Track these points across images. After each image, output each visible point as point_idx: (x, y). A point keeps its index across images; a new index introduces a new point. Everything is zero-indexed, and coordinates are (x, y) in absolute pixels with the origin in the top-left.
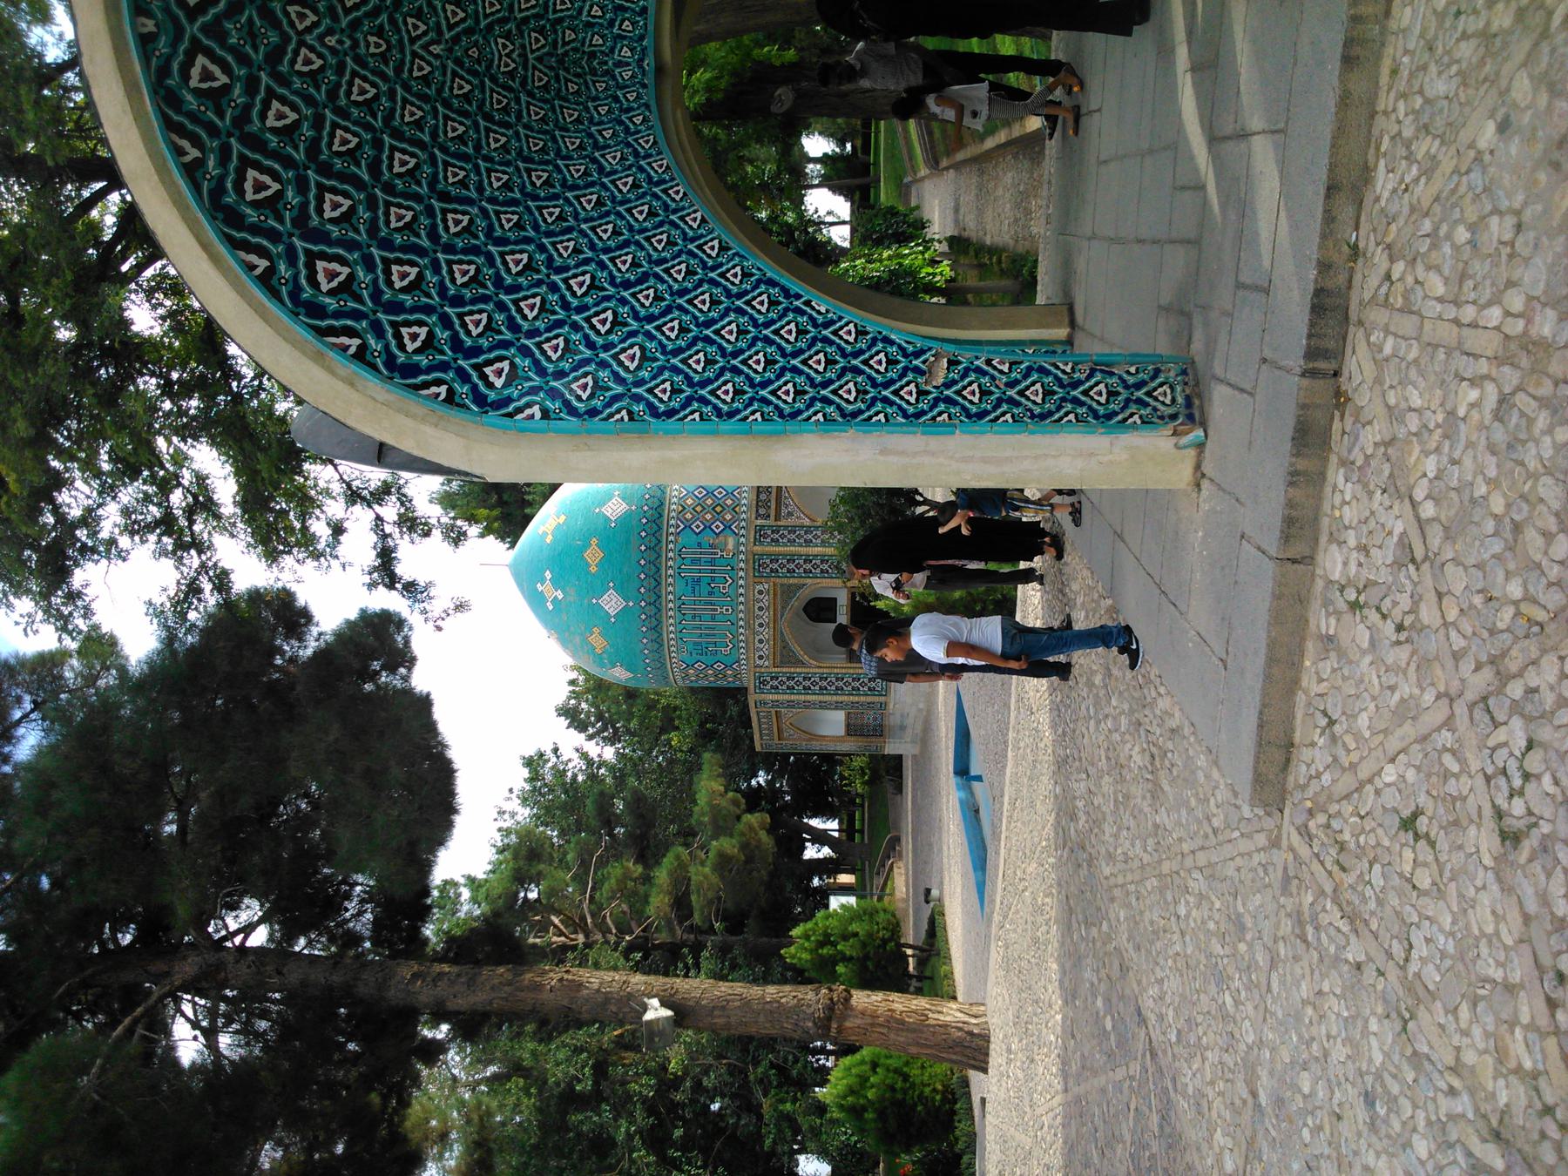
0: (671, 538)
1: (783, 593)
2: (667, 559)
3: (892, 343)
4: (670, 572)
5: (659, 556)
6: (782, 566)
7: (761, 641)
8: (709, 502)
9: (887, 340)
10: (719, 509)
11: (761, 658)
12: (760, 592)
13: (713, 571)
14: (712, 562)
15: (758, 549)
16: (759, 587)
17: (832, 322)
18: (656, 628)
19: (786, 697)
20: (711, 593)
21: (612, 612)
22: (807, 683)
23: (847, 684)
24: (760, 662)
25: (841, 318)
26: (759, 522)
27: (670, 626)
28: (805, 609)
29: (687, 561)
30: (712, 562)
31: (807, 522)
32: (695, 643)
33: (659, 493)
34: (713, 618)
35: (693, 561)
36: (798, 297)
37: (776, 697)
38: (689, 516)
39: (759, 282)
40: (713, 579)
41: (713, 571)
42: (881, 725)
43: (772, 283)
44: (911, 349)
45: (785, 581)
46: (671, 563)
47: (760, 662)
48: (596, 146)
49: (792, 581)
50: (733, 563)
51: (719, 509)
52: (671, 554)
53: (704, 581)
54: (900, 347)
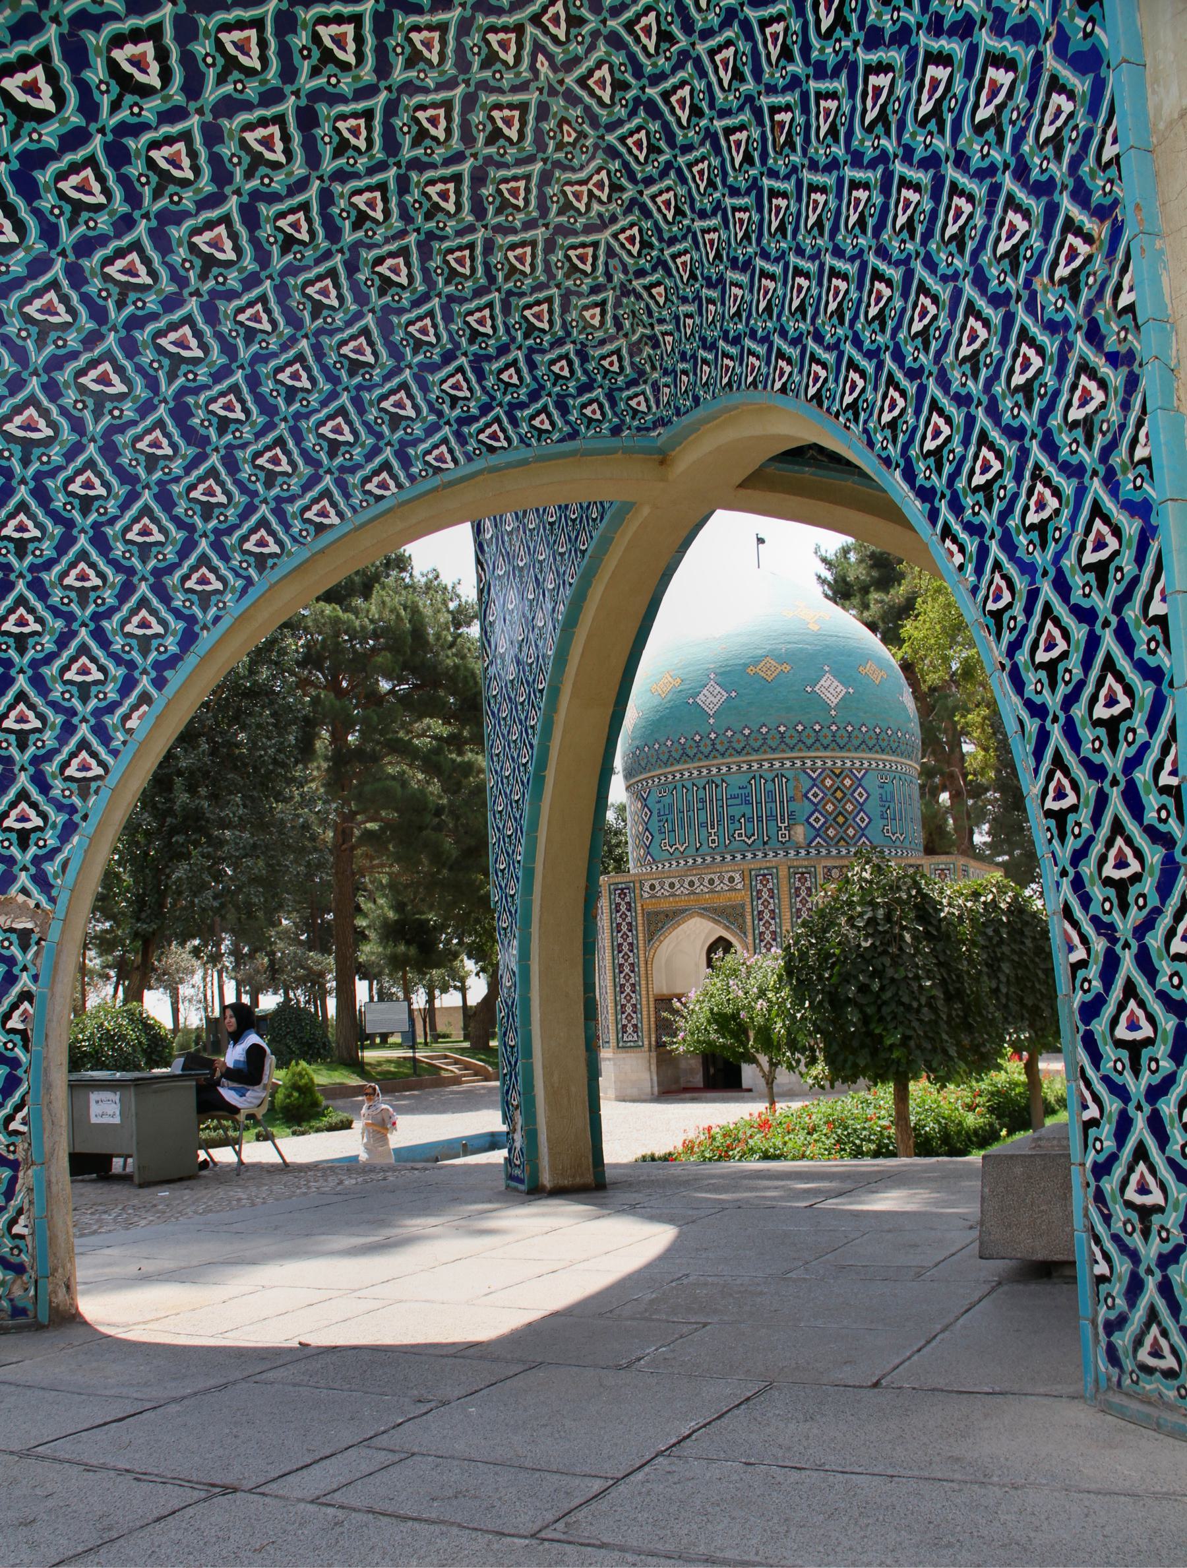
0: (798, 763)
1: (733, 907)
2: (771, 761)
3: (64, 837)
4: (755, 766)
6: (766, 904)
7: (672, 885)
8: (849, 807)
9: (69, 829)
10: (841, 820)
11: (652, 887)
12: (731, 879)
13: (760, 819)
14: (771, 817)
15: (783, 872)
16: (737, 877)
17: (106, 739)
18: (685, 756)
20: (732, 818)
21: (700, 699)
22: (625, 948)
23: (629, 998)
24: (647, 888)
25: (115, 753)
26: (820, 870)
27: (688, 770)
29: (770, 786)
32: (671, 806)
33: (856, 743)
34: (703, 825)
35: (770, 794)
36: (159, 683)
38: (828, 782)
39: (191, 620)
41: (760, 819)
43: (188, 639)
44: (50, 868)
45: (748, 909)
46: (766, 765)
47: (647, 888)
48: (478, 363)
49: (749, 918)
50: (773, 842)
51: (841, 820)
52: (777, 765)
53: (746, 809)
54: (56, 850)
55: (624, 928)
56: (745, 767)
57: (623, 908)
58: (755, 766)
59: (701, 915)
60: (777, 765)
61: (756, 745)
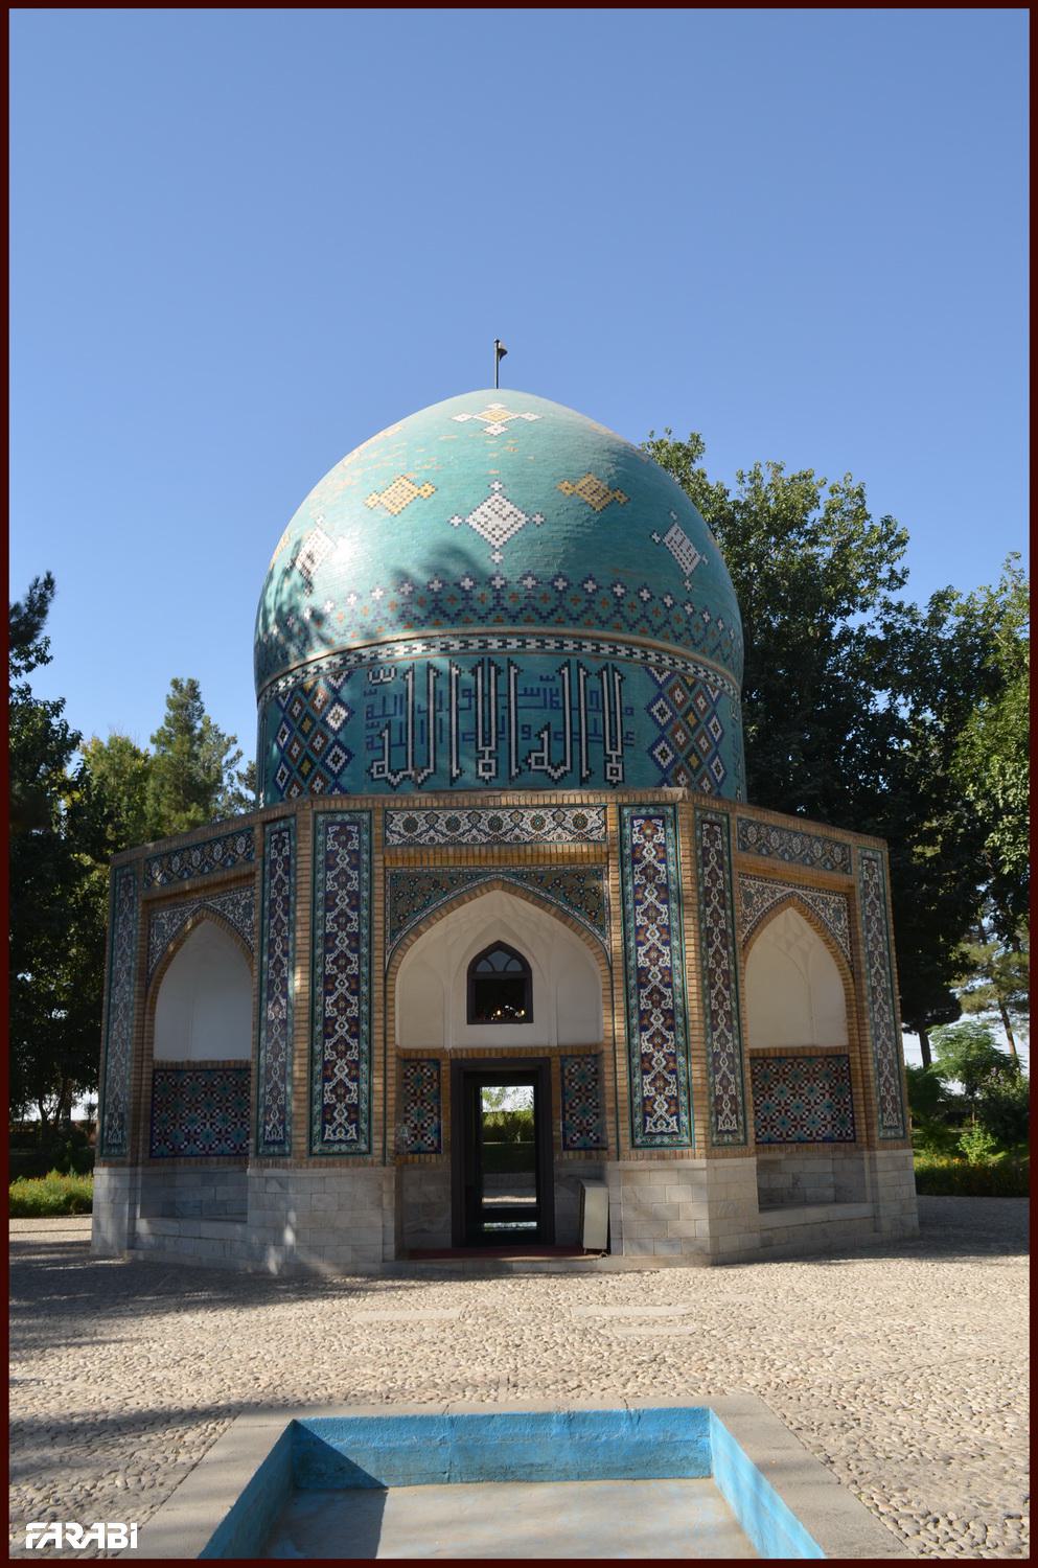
0: (639, 656)
2: (596, 641)
4: (570, 646)
5: (603, 623)
7: (453, 824)
11: (410, 825)
14: (595, 736)
19: (305, 891)
20: (525, 730)
21: (473, 521)
22: (342, 943)
24: (398, 823)
28: (499, 946)
29: (594, 682)
30: (595, 736)
31: (741, 938)
33: (711, 643)
35: (594, 697)
37: (304, 864)
38: (679, 696)
40: (558, 736)
41: (576, 737)
42: (176, 1153)
46: (589, 647)
51: (694, 761)
52: (606, 650)
55: (343, 904)
56: (552, 644)
57: (343, 862)
58: (570, 646)
59: (510, 888)
60: (606, 650)
61: (576, 609)
